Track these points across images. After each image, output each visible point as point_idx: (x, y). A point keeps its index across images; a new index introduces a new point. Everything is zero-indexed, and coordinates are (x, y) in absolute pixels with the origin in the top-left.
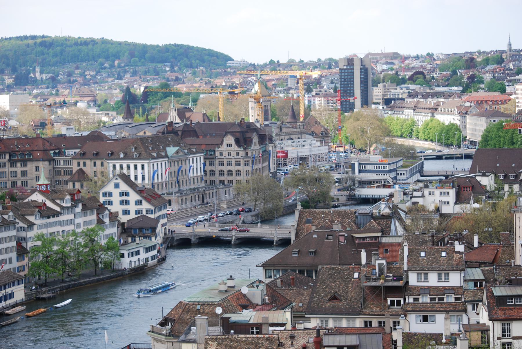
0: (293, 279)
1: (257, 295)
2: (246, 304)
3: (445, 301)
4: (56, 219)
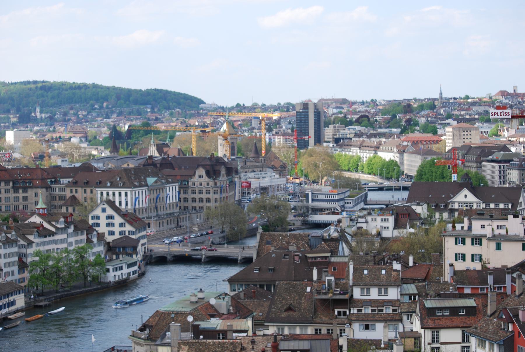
0: (254, 292)
1: (223, 306)
2: (214, 313)
3: (384, 312)
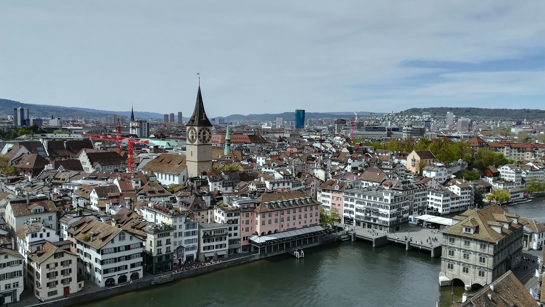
4: (537, 172)
